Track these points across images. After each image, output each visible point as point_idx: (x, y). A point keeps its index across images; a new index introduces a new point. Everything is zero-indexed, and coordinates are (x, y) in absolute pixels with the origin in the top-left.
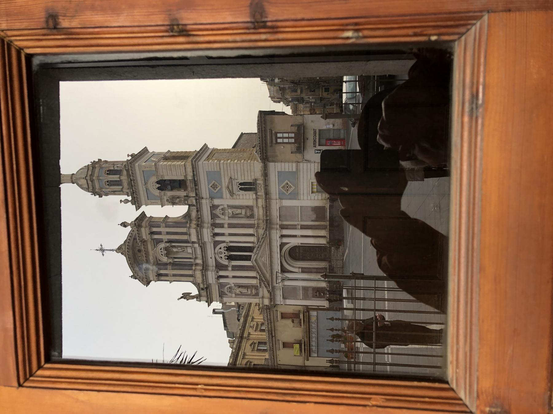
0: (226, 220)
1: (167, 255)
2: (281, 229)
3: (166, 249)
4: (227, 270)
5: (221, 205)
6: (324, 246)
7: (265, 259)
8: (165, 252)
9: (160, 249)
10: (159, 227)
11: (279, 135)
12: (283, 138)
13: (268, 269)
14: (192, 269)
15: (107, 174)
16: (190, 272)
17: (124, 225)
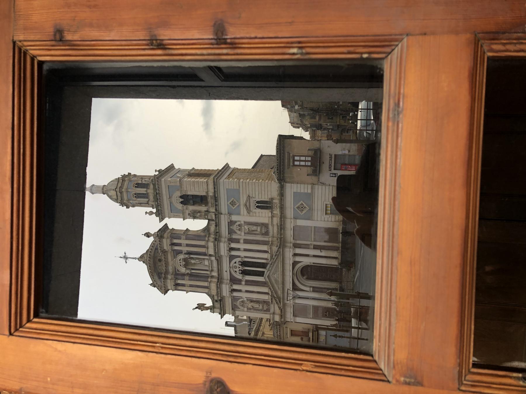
0: (241, 236)
1: (186, 266)
2: (295, 247)
3: (185, 260)
4: (240, 284)
5: (239, 221)
6: (336, 267)
8: (184, 263)
10: (179, 238)
11: (297, 158)
12: (300, 161)
13: (280, 286)
14: (208, 281)
15: (135, 187)
16: (206, 284)
17: (148, 235)
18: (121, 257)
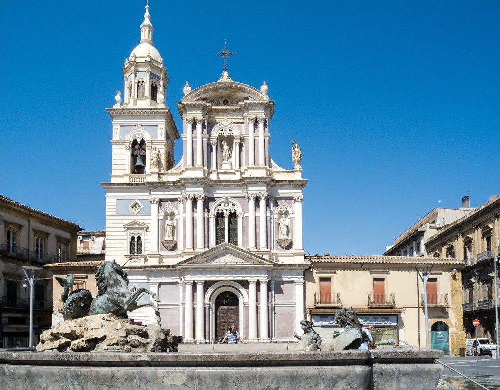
8: (226, 135)
9: (230, 129)
16: (199, 162)
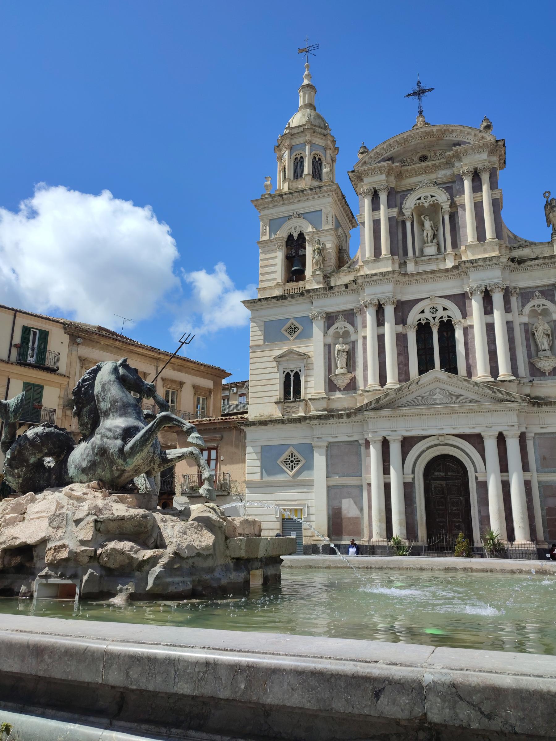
7: (438, 402)
8: (426, 205)
18: (419, 82)
